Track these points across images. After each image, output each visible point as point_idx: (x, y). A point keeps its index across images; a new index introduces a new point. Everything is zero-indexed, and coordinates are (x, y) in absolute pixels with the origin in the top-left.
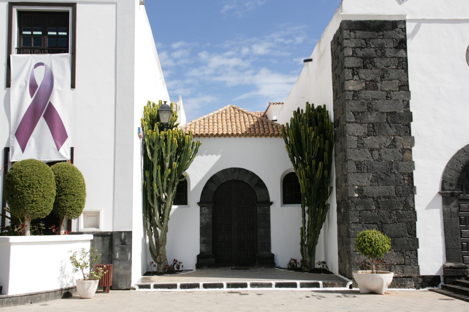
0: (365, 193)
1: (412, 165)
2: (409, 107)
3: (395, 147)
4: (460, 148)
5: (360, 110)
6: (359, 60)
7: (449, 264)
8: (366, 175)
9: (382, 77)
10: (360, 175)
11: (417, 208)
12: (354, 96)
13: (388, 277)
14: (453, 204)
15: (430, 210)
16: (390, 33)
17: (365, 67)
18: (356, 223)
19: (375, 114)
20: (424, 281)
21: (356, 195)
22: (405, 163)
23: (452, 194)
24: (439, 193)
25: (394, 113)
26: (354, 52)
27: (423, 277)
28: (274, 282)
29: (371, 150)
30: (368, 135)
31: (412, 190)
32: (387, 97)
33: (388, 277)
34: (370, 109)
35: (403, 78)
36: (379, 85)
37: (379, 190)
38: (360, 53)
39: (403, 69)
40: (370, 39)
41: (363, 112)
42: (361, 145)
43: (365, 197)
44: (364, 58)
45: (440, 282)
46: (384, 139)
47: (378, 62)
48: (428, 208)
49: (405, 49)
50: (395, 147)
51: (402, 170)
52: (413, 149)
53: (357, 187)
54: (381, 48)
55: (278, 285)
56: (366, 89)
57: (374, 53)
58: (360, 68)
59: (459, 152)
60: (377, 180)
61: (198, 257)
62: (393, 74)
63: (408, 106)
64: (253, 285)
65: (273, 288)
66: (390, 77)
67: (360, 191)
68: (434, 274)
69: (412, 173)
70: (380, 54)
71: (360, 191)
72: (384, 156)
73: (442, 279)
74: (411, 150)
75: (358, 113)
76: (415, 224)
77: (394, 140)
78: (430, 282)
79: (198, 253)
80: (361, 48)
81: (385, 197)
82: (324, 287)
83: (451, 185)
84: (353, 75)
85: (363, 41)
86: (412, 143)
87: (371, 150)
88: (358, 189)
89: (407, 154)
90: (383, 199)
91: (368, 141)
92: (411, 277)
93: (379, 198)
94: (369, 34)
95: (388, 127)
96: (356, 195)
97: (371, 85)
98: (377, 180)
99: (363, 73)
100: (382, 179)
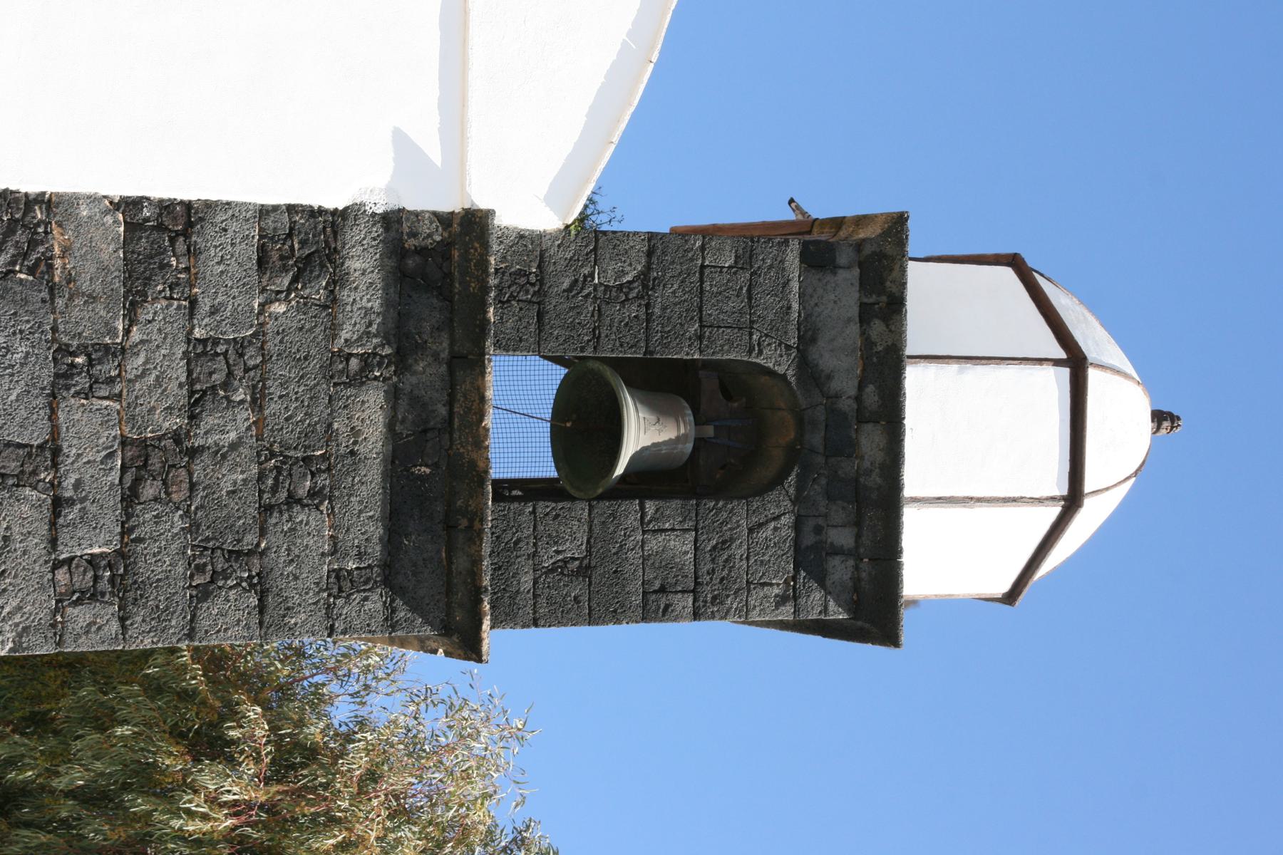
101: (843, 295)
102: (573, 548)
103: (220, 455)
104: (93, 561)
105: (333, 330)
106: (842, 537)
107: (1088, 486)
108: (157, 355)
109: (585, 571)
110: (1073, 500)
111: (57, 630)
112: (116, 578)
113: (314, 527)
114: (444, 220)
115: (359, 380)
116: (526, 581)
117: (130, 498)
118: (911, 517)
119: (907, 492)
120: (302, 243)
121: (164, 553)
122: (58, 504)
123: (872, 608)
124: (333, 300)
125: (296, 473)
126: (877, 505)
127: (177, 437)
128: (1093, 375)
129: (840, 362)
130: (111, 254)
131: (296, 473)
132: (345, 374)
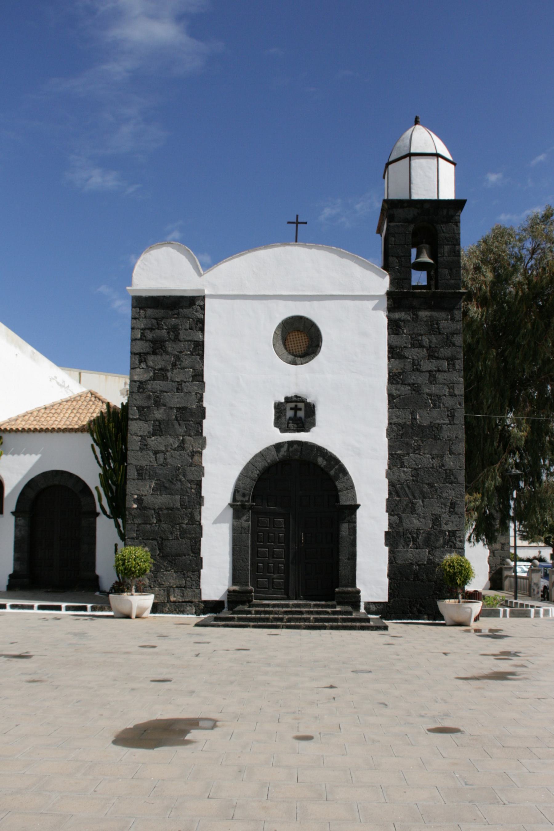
0: (145, 504)
1: (201, 471)
2: (202, 401)
3: (183, 449)
4: (257, 450)
5: (146, 404)
6: (147, 344)
7: (236, 588)
8: (147, 483)
9: (174, 365)
10: (140, 483)
11: (203, 522)
12: (139, 387)
13: (148, 600)
14: (244, 518)
15: (218, 525)
16: (185, 311)
17: (154, 353)
18: (133, 538)
19: (163, 408)
20: (205, 607)
21: (135, 506)
22: (193, 469)
23: (243, 506)
24: (230, 504)
25: (185, 408)
26: (142, 334)
27: (205, 602)
28: (36, 604)
29: (156, 453)
30: (154, 435)
31: (199, 500)
32: (178, 389)
33: (148, 600)
34: (158, 404)
35: (197, 367)
36: (169, 374)
37: (162, 500)
38: (150, 335)
39: (198, 355)
40: (163, 318)
41: (148, 407)
42: (144, 447)
43: (145, 508)
44: (154, 342)
45: (224, 608)
46: (171, 440)
47: (169, 346)
48: (215, 522)
49: (202, 330)
50: (183, 449)
51: (190, 477)
52: (204, 452)
53: (136, 496)
54: (175, 329)
55: (41, 608)
56: (154, 379)
57: (166, 335)
58: (148, 353)
59: (256, 456)
60: (161, 488)
61: (11, 576)
62: (186, 362)
63: (201, 399)
64: (13, 607)
65: (35, 611)
66: (183, 364)
67: (139, 501)
68: (217, 598)
69: (201, 481)
70: (172, 337)
71: (139, 501)
72: (169, 460)
73: (226, 605)
74: (201, 453)
75: (143, 408)
76: (200, 541)
77: (183, 441)
78: (213, 607)
79: (11, 572)
80: (151, 329)
81: (168, 509)
82: (92, 611)
83: (244, 495)
84: (140, 362)
85: (154, 321)
86: (203, 444)
87: (156, 453)
88: (137, 499)
89: (196, 458)
90: (165, 512)
91: (153, 441)
92: (191, 602)
93: (161, 509)
94: (160, 313)
95: (177, 426)
96: (135, 506)
97: (161, 374)
98: (161, 488)
99: (151, 360)
100: (166, 487)
101: (399, 213)
102: (446, 272)
103: (430, 342)
104: (448, 365)
105: (409, 321)
106: (445, 212)
107: (435, 152)
108: (414, 353)
109: (451, 269)
110: (437, 155)
111: (459, 371)
112: (451, 360)
113: (443, 324)
114: (388, 299)
115: (417, 316)
116: (453, 281)
117: (438, 358)
118: (441, 198)
119: (435, 198)
120: (394, 327)
121: (446, 352)
122: (439, 371)
123: (457, 205)
124: (403, 321)
125: (433, 327)
126: (438, 205)
127: (427, 350)
128: (413, 151)
129: (412, 213)
130: (397, 361)
131: (433, 327)
132: (416, 319)
